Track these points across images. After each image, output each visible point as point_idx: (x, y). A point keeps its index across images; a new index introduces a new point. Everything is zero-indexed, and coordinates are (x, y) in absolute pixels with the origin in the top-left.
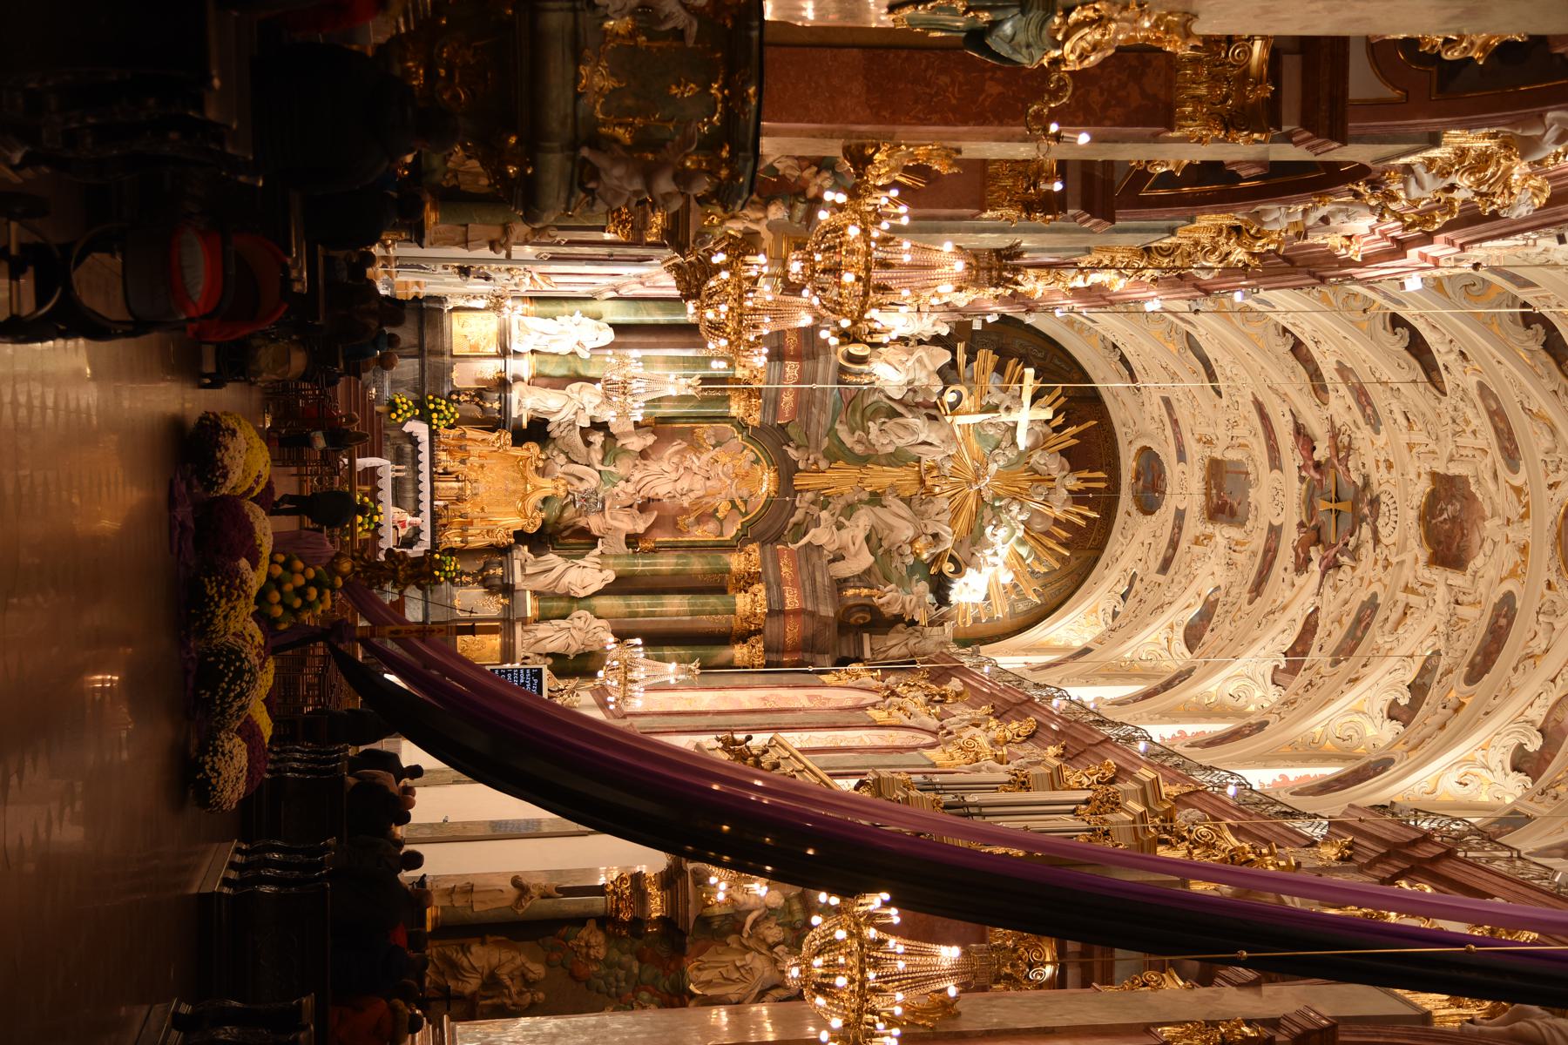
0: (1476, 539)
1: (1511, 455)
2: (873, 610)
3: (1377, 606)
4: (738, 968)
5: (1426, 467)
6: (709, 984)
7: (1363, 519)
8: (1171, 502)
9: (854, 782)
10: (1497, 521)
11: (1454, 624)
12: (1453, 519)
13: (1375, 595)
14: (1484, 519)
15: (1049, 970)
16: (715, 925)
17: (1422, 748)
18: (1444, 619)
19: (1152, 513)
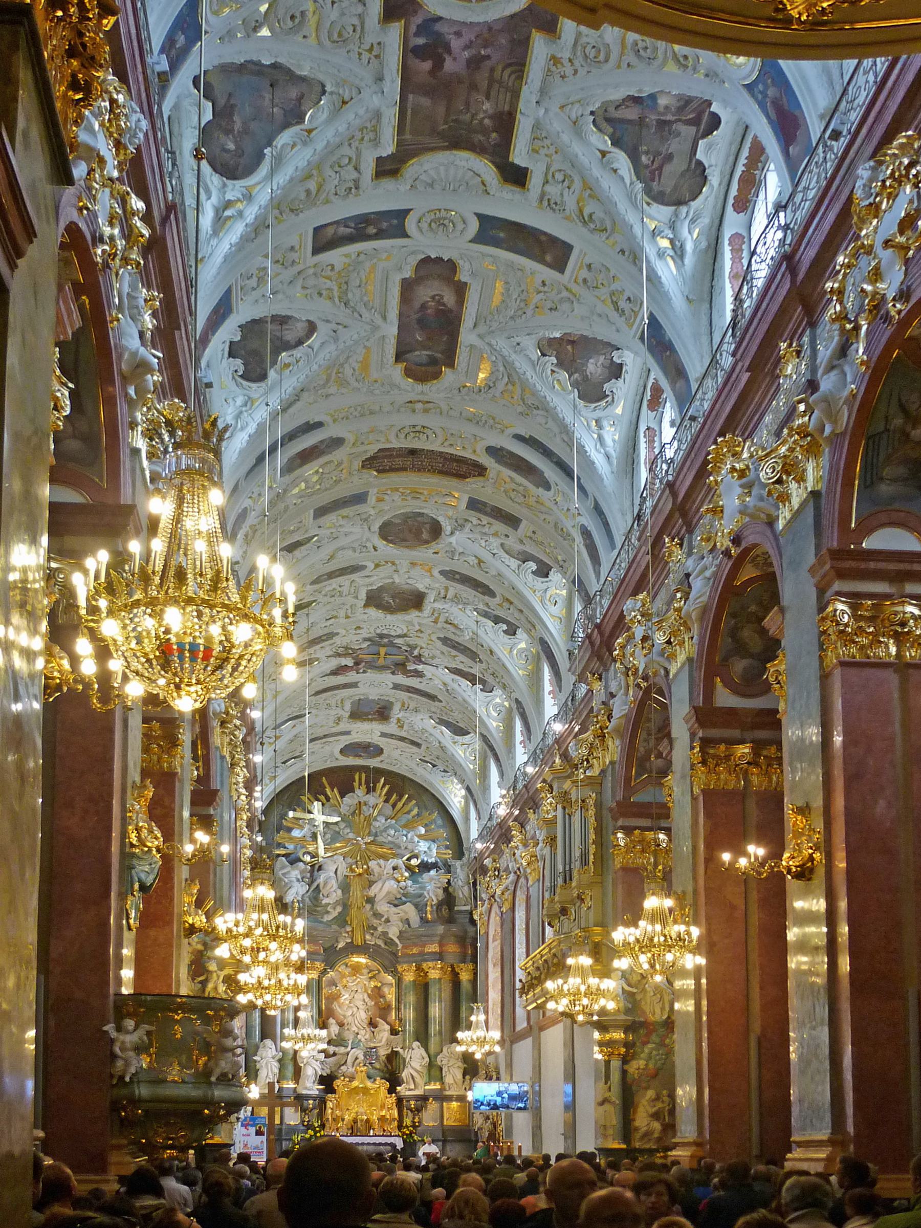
0: (407, 587)
1: (355, 569)
2: (440, 904)
3: (445, 638)
4: (655, 995)
5: (361, 610)
6: (662, 1009)
7: (391, 642)
8: (377, 739)
9: (547, 928)
10: (396, 576)
11: (457, 599)
12: (393, 597)
13: (439, 638)
14: (393, 583)
15: (662, 836)
16: (630, 1006)
17: (533, 624)
18: (454, 605)
19: (382, 749)
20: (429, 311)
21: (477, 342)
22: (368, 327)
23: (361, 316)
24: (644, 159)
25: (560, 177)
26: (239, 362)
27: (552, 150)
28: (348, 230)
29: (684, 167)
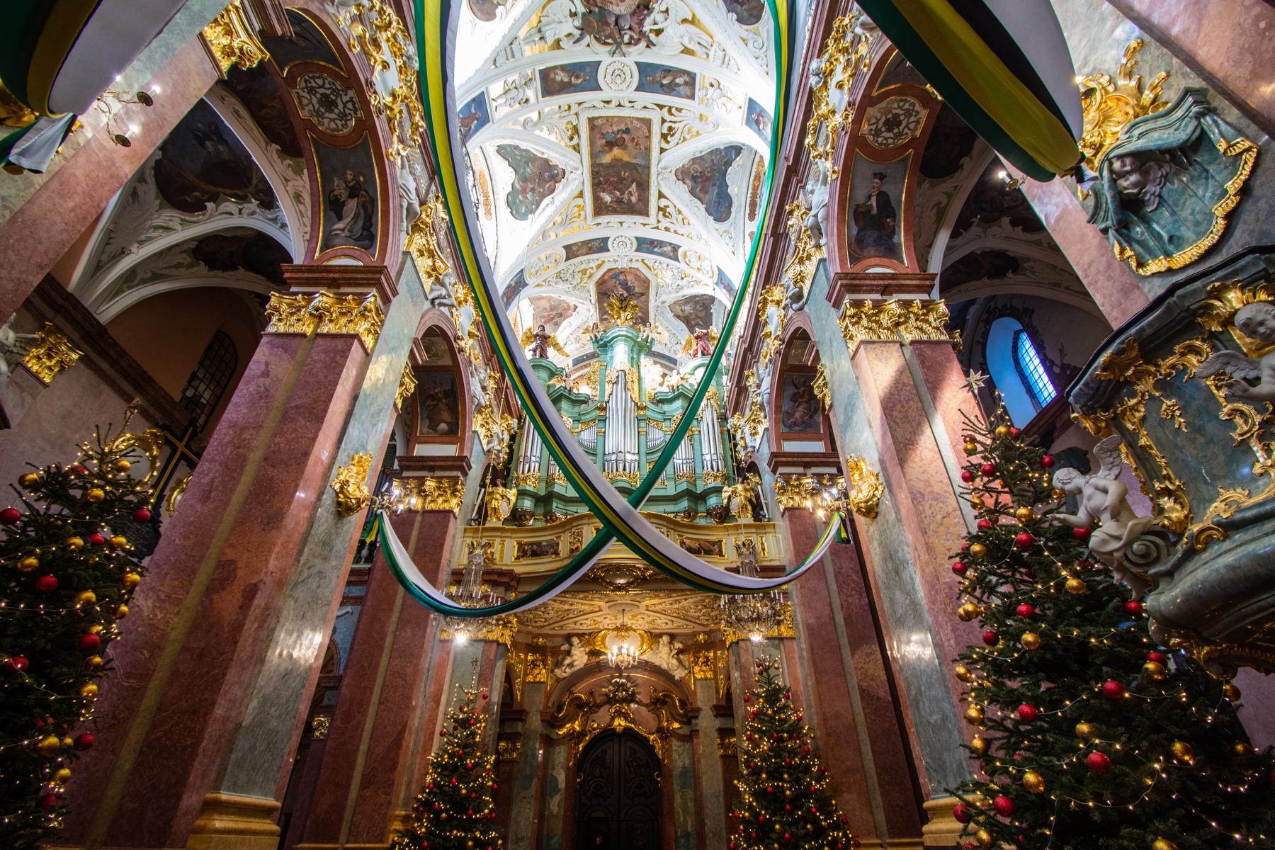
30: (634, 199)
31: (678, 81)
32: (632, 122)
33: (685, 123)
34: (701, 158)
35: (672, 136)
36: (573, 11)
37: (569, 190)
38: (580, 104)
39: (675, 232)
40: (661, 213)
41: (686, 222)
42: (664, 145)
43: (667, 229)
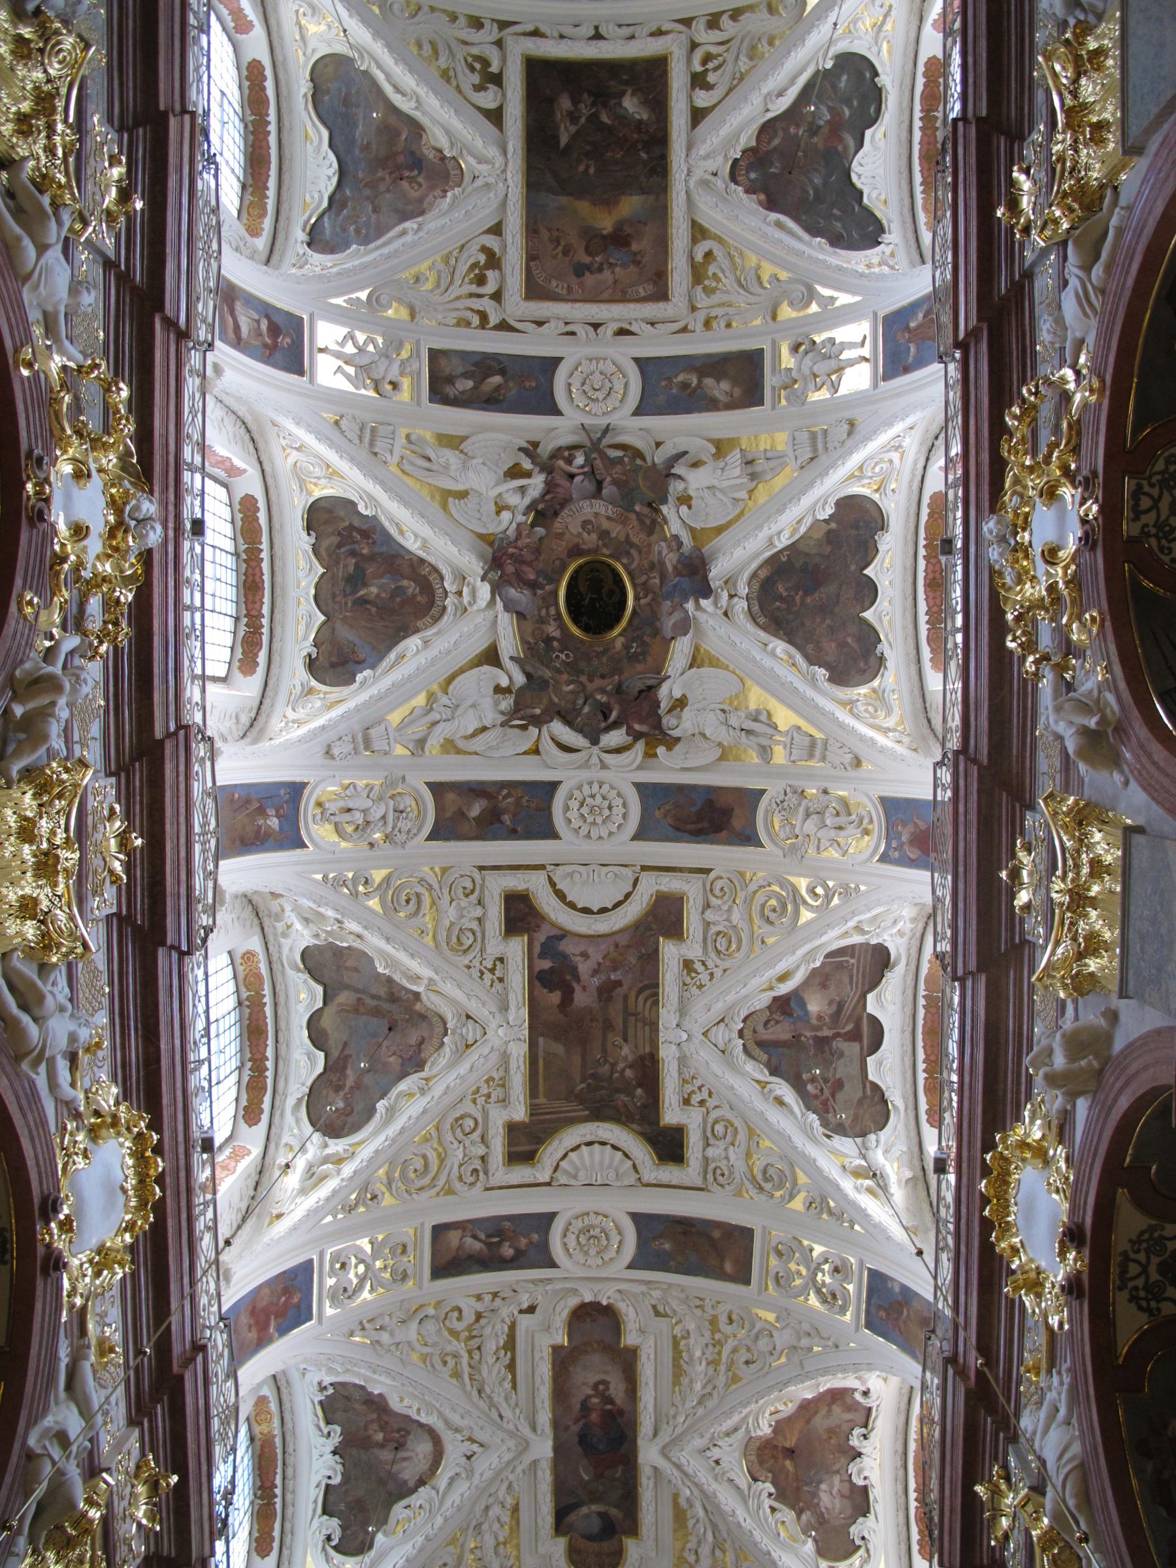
20: (594, 1416)
21: (661, 1463)
22: (511, 1443)
23: (501, 1417)
24: (809, 1087)
25: (719, 1128)
26: (335, 1522)
27: (705, 1095)
28: (478, 1246)
29: (860, 1094)
30: (565, 103)
31: (470, 384)
32: (570, 290)
33: (448, 297)
34: (405, 218)
35: (475, 265)
36: (684, 509)
37: (724, 131)
38: (684, 330)
39: (454, 18)
40: (494, 69)
41: (427, 50)
42: (492, 242)
43: (477, 23)
